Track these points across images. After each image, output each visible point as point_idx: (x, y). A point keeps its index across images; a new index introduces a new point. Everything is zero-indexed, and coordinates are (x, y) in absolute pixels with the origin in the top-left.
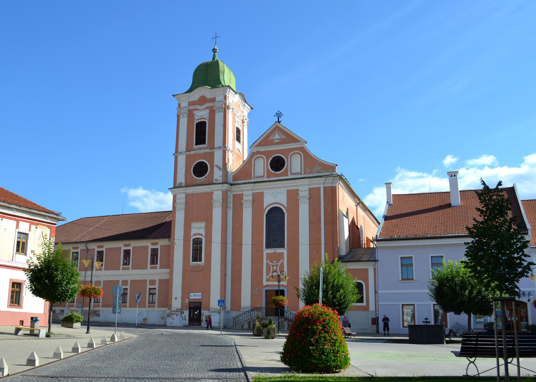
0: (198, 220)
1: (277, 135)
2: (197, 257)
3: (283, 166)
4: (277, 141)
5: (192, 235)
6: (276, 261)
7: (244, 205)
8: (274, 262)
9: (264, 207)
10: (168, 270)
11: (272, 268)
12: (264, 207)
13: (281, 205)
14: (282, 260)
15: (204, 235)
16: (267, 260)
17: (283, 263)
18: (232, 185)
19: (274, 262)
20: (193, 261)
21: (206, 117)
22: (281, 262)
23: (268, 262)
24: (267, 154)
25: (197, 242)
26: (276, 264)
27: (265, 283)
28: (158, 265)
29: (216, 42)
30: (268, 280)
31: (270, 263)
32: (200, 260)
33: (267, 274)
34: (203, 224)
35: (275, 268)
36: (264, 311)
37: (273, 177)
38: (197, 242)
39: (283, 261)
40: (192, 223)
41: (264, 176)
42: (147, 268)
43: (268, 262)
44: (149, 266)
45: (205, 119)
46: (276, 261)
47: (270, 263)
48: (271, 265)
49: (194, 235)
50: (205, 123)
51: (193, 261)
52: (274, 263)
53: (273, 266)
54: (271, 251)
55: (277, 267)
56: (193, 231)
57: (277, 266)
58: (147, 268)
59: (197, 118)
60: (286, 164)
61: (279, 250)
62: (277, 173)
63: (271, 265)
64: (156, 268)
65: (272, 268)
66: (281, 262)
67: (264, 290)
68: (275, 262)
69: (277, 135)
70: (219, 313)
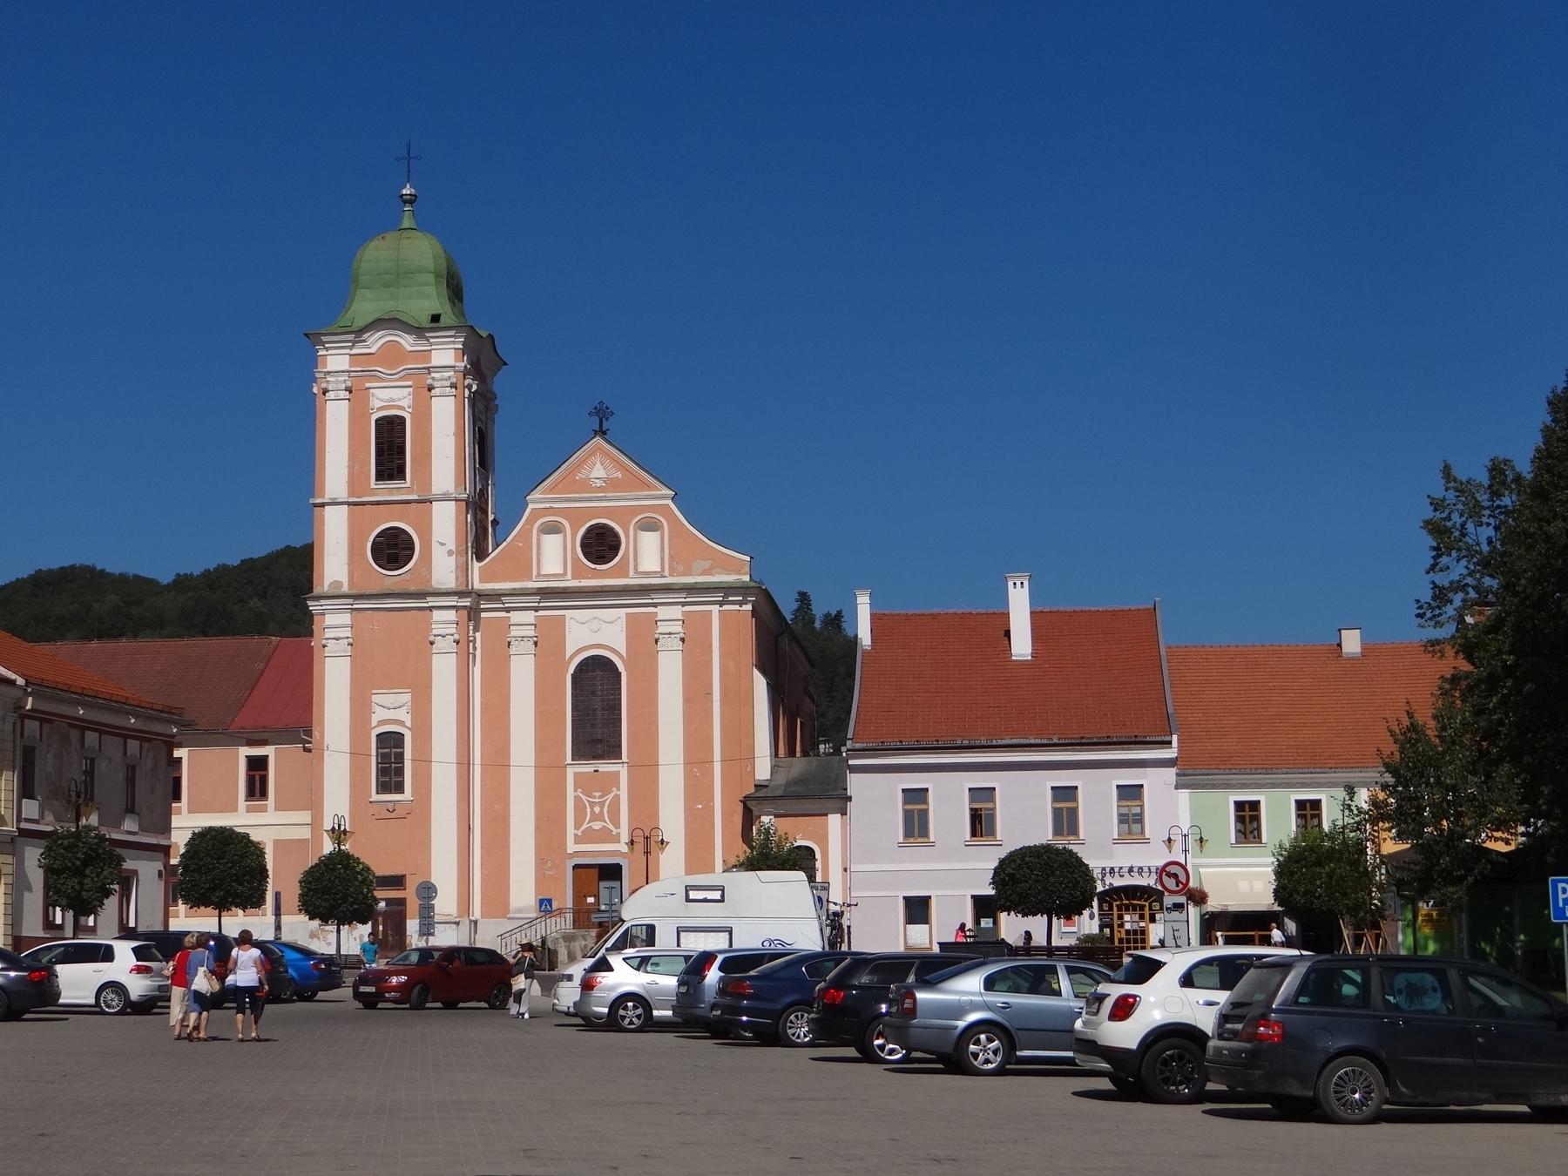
0: (392, 683)
1: (598, 465)
2: (390, 778)
3: (615, 548)
4: (599, 483)
5: (374, 721)
6: (600, 794)
7: (513, 650)
8: (595, 794)
9: (568, 655)
10: (305, 817)
11: (588, 810)
12: (568, 655)
13: (613, 652)
14: (614, 789)
15: (409, 724)
16: (576, 791)
17: (617, 798)
18: (480, 595)
19: (595, 794)
20: (377, 793)
21: (405, 403)
22: (613, 794)
23: (581, 795)
24: (575, 517)
25: (390, 743)
26: (601, 800)
27: (571, 847)
28: (271, 800)
29: (409, 172)
30: (578, 840)
31: (583, 797)
32: (399, 788)
33: (577, 827)
34: (406, 698)
35: (597, 810)
36: (569, 917)
37: (589, 578)
38: (390, 743)
39: (618, 793)
40: (373, 691)
41: (565, 573)
42: (235, 810)
43: (581, 795)
44: (242, 803)
45: (402, 408)
46: (600, 794)
47: (583, 797)
48: (587, 803)
49: (381, 723)
50: (401, 421)
51: (377, 793)
52: (595, 797)
53: (592, 805)
54: (587, 768)
55: (602, 808)
56: (379, 715)
57: (602, 804)
58: (235, 810)
59: (375, 403)
60: (623, 546)
61: (606, 767)
62: (598, 567)
63: (587, 803)
64: (264, 810)
65: (588, 810)
66: (613, 794)
67: (570, 864)
68: (598, 794)
69: (598, 465)
70: (458, 923)
